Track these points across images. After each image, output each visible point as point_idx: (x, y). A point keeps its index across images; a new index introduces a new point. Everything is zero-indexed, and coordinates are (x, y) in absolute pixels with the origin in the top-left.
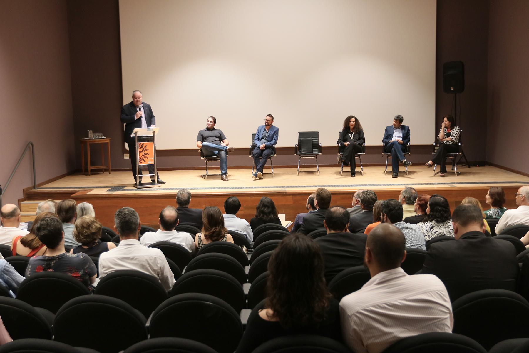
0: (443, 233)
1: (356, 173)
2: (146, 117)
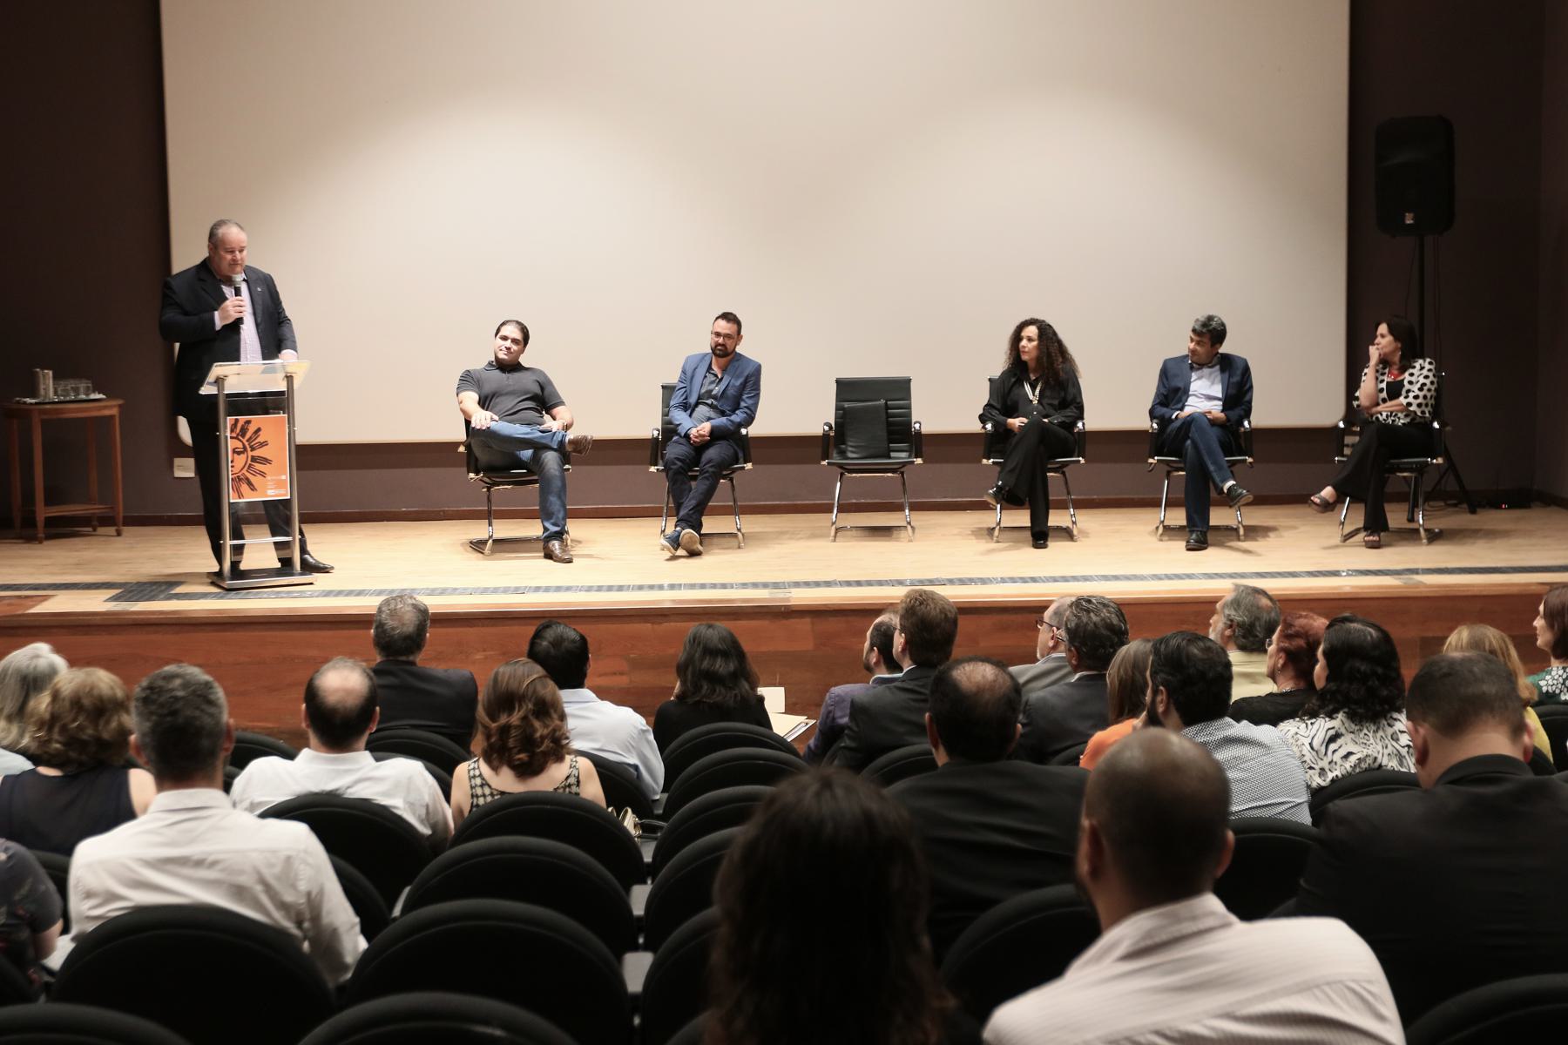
0: (1376, 758)
1: (1050, 534)
2: (259, 320)
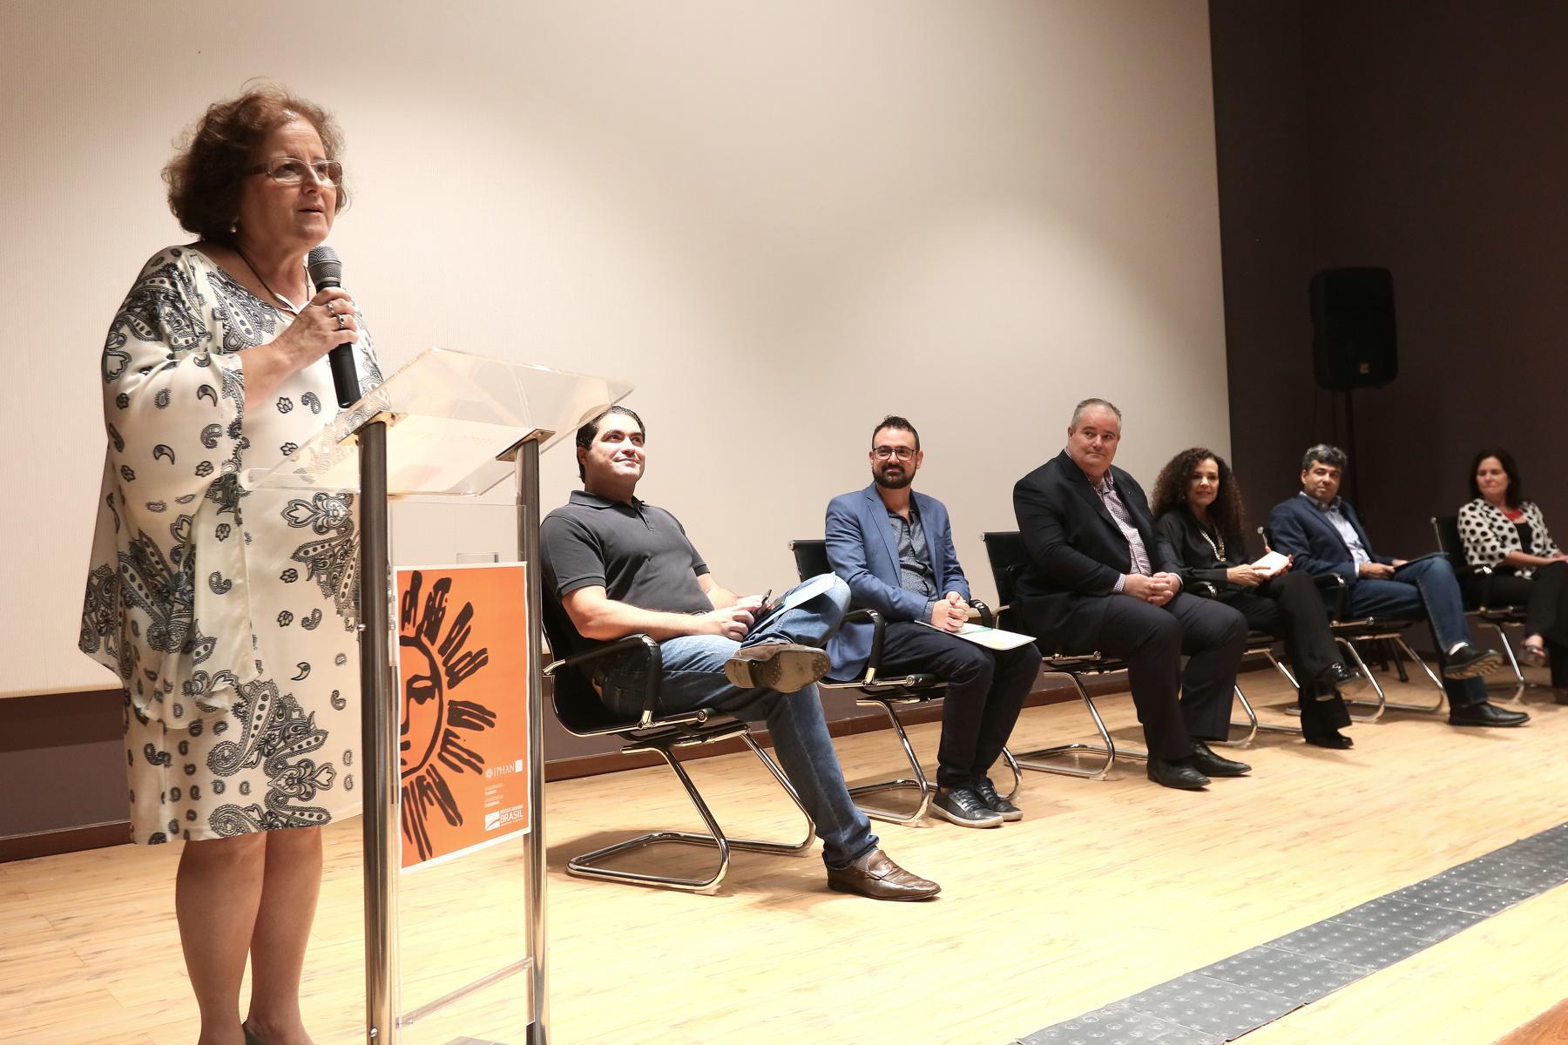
1: (1231, 733)
